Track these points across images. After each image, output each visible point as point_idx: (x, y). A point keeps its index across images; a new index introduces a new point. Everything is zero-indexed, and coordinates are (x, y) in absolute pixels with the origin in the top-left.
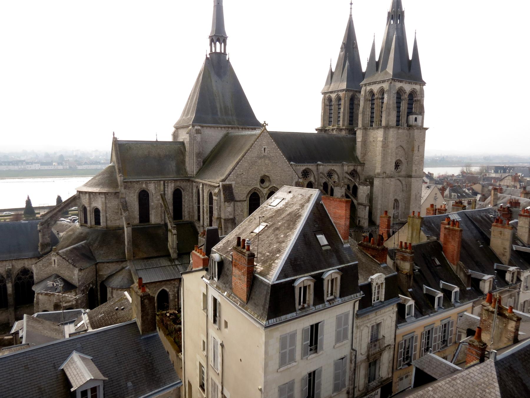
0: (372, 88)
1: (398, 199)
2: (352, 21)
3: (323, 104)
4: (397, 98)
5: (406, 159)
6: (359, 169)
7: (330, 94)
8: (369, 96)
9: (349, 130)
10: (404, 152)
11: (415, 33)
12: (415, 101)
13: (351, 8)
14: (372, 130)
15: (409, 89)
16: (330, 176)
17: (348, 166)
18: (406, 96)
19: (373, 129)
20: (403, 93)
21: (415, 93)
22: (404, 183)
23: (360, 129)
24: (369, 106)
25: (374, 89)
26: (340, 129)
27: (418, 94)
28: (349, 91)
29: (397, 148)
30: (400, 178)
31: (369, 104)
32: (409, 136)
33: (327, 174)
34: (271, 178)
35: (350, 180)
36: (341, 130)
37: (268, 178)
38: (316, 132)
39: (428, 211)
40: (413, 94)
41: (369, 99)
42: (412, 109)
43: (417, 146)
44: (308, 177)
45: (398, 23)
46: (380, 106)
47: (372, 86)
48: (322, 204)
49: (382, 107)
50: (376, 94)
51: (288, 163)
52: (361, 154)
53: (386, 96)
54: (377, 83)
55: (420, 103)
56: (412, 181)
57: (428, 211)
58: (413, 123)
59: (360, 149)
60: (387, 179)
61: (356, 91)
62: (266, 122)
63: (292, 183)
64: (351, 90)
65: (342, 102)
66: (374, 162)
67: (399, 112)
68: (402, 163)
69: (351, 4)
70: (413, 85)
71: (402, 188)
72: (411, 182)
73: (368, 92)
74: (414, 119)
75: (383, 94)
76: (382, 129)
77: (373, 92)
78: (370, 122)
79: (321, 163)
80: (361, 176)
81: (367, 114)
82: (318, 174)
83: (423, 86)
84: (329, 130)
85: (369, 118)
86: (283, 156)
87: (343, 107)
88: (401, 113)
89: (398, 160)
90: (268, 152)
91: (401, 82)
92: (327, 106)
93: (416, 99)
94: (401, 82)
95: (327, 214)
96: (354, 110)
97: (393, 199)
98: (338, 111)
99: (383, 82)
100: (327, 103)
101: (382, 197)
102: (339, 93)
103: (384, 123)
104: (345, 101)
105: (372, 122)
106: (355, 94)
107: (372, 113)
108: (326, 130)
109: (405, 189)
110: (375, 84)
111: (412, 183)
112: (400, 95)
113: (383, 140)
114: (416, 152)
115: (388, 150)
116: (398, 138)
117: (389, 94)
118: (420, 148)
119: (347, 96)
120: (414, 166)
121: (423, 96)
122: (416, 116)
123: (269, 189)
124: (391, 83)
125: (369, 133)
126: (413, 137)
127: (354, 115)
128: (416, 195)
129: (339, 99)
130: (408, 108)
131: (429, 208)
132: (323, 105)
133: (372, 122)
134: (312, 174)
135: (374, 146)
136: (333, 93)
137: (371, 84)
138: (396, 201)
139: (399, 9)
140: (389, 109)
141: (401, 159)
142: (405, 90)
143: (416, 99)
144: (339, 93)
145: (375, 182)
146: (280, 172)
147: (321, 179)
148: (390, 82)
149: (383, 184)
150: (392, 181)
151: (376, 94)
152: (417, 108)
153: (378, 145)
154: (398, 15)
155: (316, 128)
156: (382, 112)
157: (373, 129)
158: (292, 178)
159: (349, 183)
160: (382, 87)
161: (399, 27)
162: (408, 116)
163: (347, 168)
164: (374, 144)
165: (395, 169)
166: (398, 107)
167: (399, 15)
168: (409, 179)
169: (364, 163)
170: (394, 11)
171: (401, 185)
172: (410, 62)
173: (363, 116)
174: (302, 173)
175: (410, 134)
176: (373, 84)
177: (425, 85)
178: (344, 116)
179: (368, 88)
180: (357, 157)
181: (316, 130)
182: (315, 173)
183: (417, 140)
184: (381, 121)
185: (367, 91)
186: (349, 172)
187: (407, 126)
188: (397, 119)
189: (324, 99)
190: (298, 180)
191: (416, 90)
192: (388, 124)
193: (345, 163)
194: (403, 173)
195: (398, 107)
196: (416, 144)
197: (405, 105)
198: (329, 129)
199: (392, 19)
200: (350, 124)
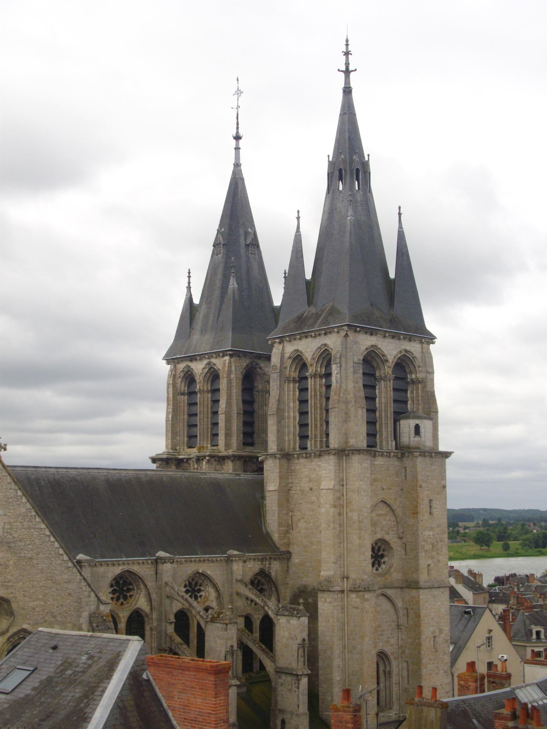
0: (300, 349)
1: (388, 650)
2: (242, 179)
3: (171, 389)
4: (364, 374)
5: (401, 538)
6: (275, 568)
7: (190, 364)
8: (293, 368)
9: (245, 461)
10: (393, 519)
11: (400, 214)
12: (413, 382)
13: (237, 149)
14: (306, 460)
15: (395, 353)
16: (194, 591)
17: (245, 562)
18: (388, 370)
19: (306, 458)
20: (379, 360)
21: (410, 363)
22: (400, 604)
23: (273, 456)
24: (294, 395)
25: (303, 351)
26: (219, 457)
27: (417, 364)
28: (239, 356)
29: (374, 507)
30: (389, 592)
31: (294, 391)
32: (403, 474)
33: (185, 586)
34: (14, 605)
35: (252, 601)
36: (221, 460)
37: (6, 606)
38: (154, 466)
39: (462, 683)
40: (404, 364)
41: (294, 378)
42: (406, 402)
43: (426, 502)
44: (131, 596)
45: (357, 188)
46: (324, 394)
48: (148, 680)
49: (328, 399)
50: (311, 365)
51: (66, 558)
52: (280, 525)
53: (334, 368)
54: (311, 336)
55: (425, 387)
56: (421, 597)
57: (462, 683)
58: (412, 439)
59: (277, 512)
60: (354, 595)
61: (259, 357)
63: (80, 617)
64: (245, 354)
65: (223, 384)
66: (314, 547)
67: (371, 411)
68: (391, 548)
69: (238, 138)
70: (402, 342)
71: (395, 618)
72: (418, 602)
73: (290, 358)
74: (413, 429)
75: (328, 365)
76: (332, 457)
77: (302, 359)
78: (298, 438)
79: (167, 555)
80: (281, 589)
81: (289, 417)
82: (160, 588)
83: (429, 343)
84: (188, 459)
85: (294, 427)
86: (52, 539)
87: (225, 398)
88: (377, 414)
89: (380, 540)
90: (7, 526)
91: (372, 333)
92: (183, 394)
93: (413, 376)
94: (371, 334)
95: (164, 709)
96: (256, 406)
97: (374, 652)
98: (212, 407)
99: (325, 334)
100: (183, 387)
101: (344, 647)
102: (213, 360)
103: (334, 442)
104: (229, 381)
105: (304, 437)
106: (257, 364)
107: (303, 413)
108: (182, 460)
109: (403, 620)
110: (306, 337)
111: (421, 603)
112: (373, 367)
113: (334, 485)
114: (424, 516)
115: (350, 514)
116: (375, 480)
117: (343, 365)
118: (434, 505)
119: (236, 370)
120: (422, 554)
121: (430, 370)
122: (417, 421)
123: (8, 639)
124: (346, 335)
125: (298, 467)
126: (415, 477)
127: (256, 419)
128: (435, 637)
130: (395, 401)
131: (463, 674)
132: (171, 392)
133: (304, 437)
134: (142, 586)
135: (312, 503)
136: (196, 360)
137: (295, 339)
138: (382, 656)
139: (354, 157)
140: (347, 403)
141: (387, 538)
142: (384, 355)
143: (413, 376)
144: (213, 360)
145: (320, 605)
146: (41, 584)
147: (167, 601)
148: (343, 333)
149: (343, 608)
150: (367, 600)
151: (311, 365)
152: (418, 400)
153: (322, 501)
154: (355, 171)
155: (153, 454)
156: (327, 411)
157: (308, 456)
158: (79, 601)
159: (252, 612)
160: (326, 345)
161: (359, 199)
162: (396, 421)
163: (241, 568)
164: (314, 499)
165: (373, 565)
166: (370, 399)
167: (358, 170)
168: (414, 592)
169: (289, 553)
170: (344, 161)
171: (392, 610)
172: (390, 285)
173: (279, 422)
174: (112, 586)
175: (405, 468)
176: (300, 339)
177: (433, 343)
178: (228, 421)
179: (290, 348)
180: (268, 533)
181: (154, 460)
182: (150, 584)
183: (424, 485)
184: (327, 435)
185: (287, 355)
186: (247, 579)
187: (396, 449)
188: (367, 429)
189: (173, 375)
190: (98, 607)
191: (412, 354)
192: (347, 442)
193: (236, 552)
194: (396, 576)
195: (370, 399)
196: (424, 495)
197: (386, 392)
198: (190, 459)
199: (341, 178)
200: (245, 444)
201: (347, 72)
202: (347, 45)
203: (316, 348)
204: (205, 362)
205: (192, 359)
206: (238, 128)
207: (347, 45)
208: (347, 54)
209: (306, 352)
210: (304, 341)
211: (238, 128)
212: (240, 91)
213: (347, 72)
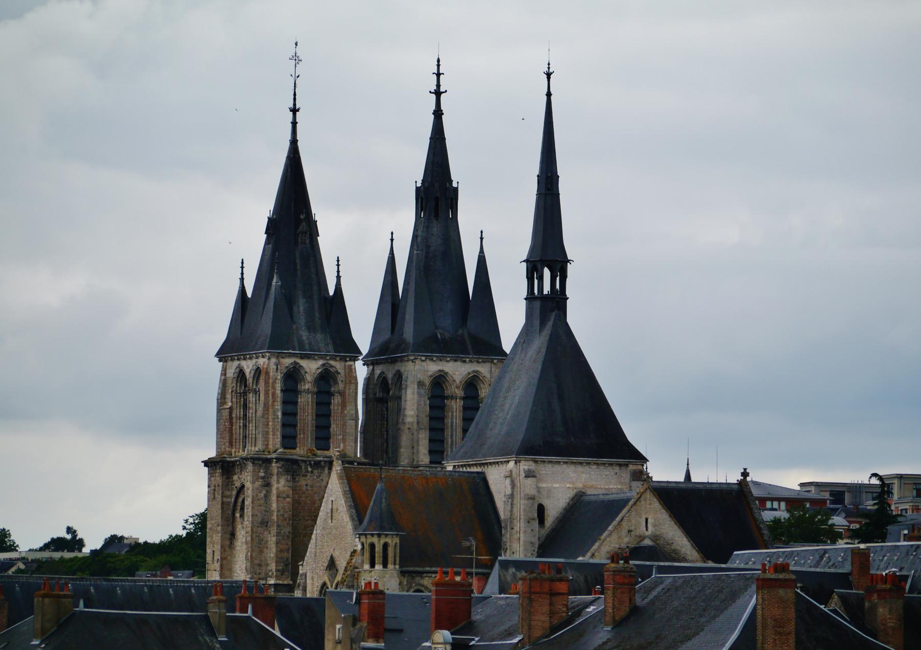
13: (294, 124)
25: (450, 373)
45: (451, 217)
47: (445, 363)
62: (748, 471)
69: (294, 110)
102: (332, 363)
110: (456, 361)
129: (326, 378)
144: (332, 363)
179: (433, 367)
201: (438, 93)
202: (438, 66)
203: (466, 372)
204: (321, 362)
205: (303, 357)
206: (295, 99)
207: (438, 66)
208: (438, 75)
209: (453, 374)
210: (451, 364)
211: (295, 99)
212: (298, 57)
213: (438, 93)
